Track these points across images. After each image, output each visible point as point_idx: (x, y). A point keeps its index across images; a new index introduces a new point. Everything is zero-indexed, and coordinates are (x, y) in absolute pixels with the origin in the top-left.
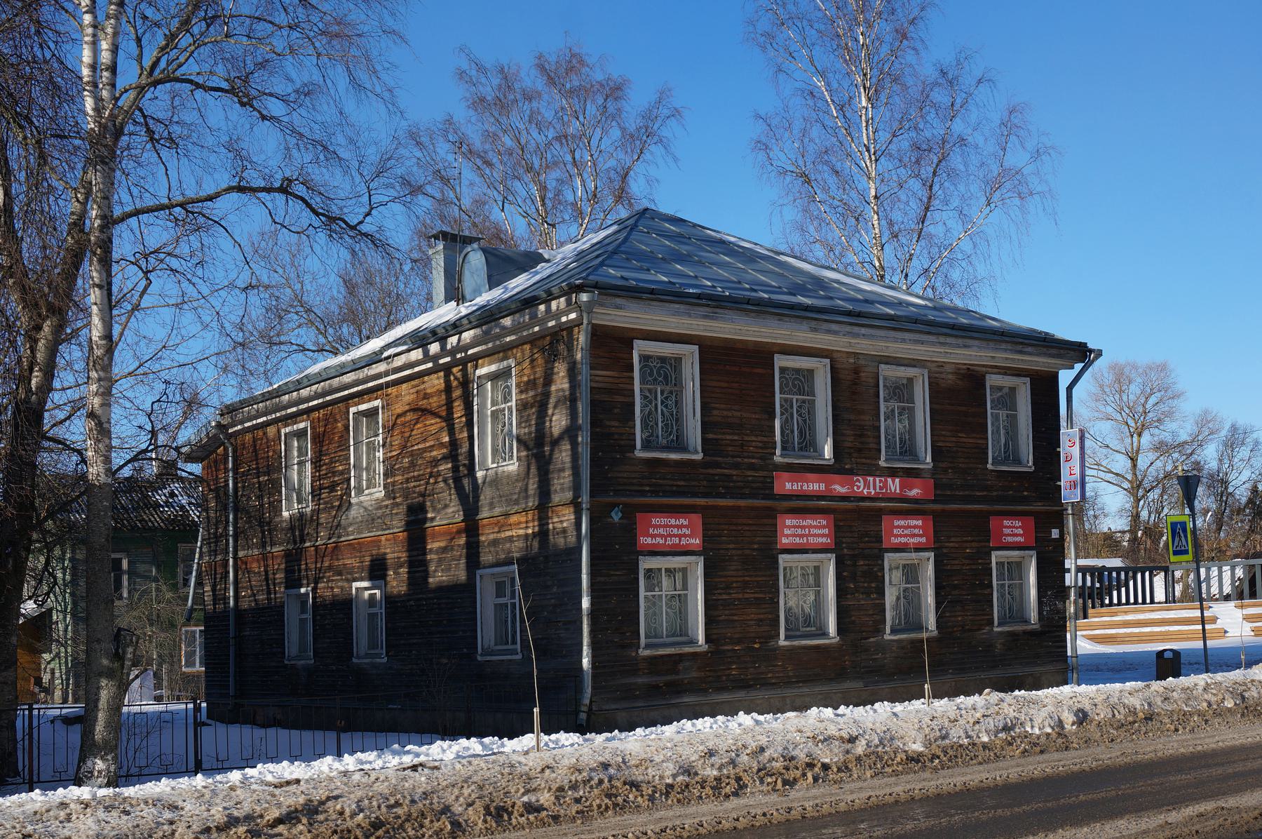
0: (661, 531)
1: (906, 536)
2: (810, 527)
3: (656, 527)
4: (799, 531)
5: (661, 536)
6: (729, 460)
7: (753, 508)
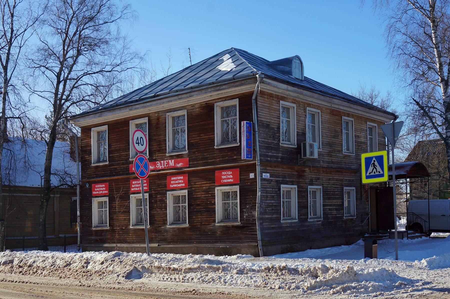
0: (98, 189)
1: (176, 184)
3: (97, 188)
4: (137, 186)
5: (98, 191)
6: (116, 162)
7: (123, 179)
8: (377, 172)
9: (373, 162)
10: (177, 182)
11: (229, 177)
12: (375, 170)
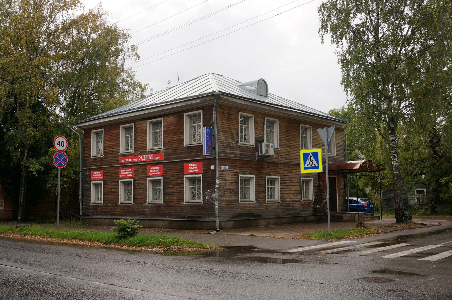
0: (95, 175)
1: (154, 172)
2: (127, 172)
4: (125, 173)
5: (95, 176)
8: (313, 165)
9: (309, 157)
10: (154, 171)
11: (194, 168)
12: (311, 163)
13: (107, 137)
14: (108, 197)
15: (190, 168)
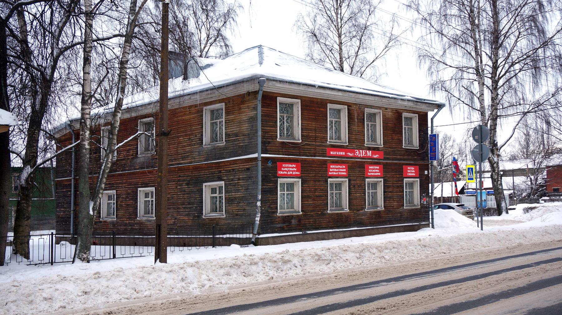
0: (286, 169)
1: (373, 172)
2: (339, 168)
4: (335, 170)
5: (286, 171)
10: (374, 171)
13: (306, 114)
14: (309, 202)
15: (409, 171)
